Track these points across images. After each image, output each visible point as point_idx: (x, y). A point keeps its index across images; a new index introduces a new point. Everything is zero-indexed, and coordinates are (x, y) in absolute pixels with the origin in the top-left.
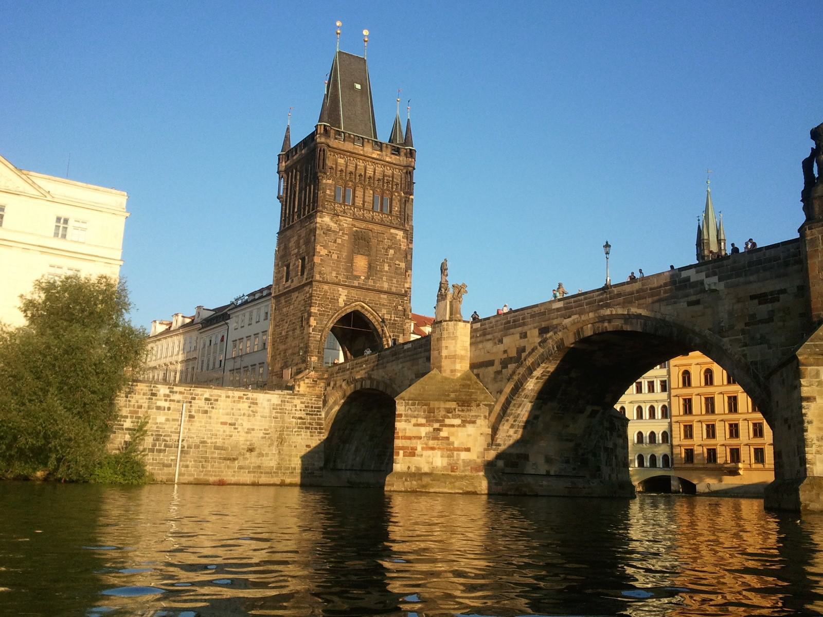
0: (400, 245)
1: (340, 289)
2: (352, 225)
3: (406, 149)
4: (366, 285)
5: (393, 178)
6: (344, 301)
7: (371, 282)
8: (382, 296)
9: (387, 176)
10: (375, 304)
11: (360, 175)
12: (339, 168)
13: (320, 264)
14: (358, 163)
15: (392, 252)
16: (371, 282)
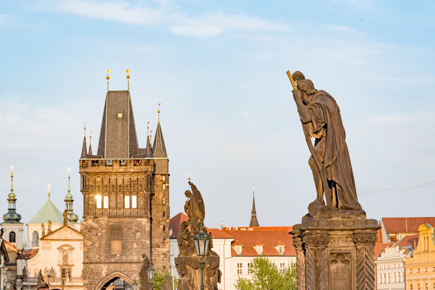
0: (145, 228)
1: (102, 265)
2: (108, 221)
3: (145, 160)
4: (121, 260)
5: (138, 181)
6: (105, 273)
7: (124, 258)
8: (133, 265)
9: (133, 181)
10: (128, 271)
11: (113, 186)
12: (97, 185)
13: (87, 252)
14: (111, 178)
15: (138, 234)
16: (124, 258)
